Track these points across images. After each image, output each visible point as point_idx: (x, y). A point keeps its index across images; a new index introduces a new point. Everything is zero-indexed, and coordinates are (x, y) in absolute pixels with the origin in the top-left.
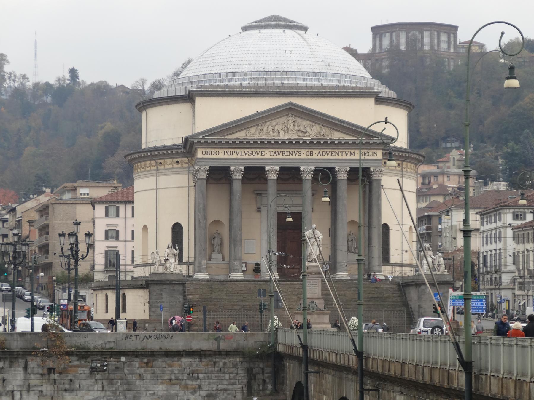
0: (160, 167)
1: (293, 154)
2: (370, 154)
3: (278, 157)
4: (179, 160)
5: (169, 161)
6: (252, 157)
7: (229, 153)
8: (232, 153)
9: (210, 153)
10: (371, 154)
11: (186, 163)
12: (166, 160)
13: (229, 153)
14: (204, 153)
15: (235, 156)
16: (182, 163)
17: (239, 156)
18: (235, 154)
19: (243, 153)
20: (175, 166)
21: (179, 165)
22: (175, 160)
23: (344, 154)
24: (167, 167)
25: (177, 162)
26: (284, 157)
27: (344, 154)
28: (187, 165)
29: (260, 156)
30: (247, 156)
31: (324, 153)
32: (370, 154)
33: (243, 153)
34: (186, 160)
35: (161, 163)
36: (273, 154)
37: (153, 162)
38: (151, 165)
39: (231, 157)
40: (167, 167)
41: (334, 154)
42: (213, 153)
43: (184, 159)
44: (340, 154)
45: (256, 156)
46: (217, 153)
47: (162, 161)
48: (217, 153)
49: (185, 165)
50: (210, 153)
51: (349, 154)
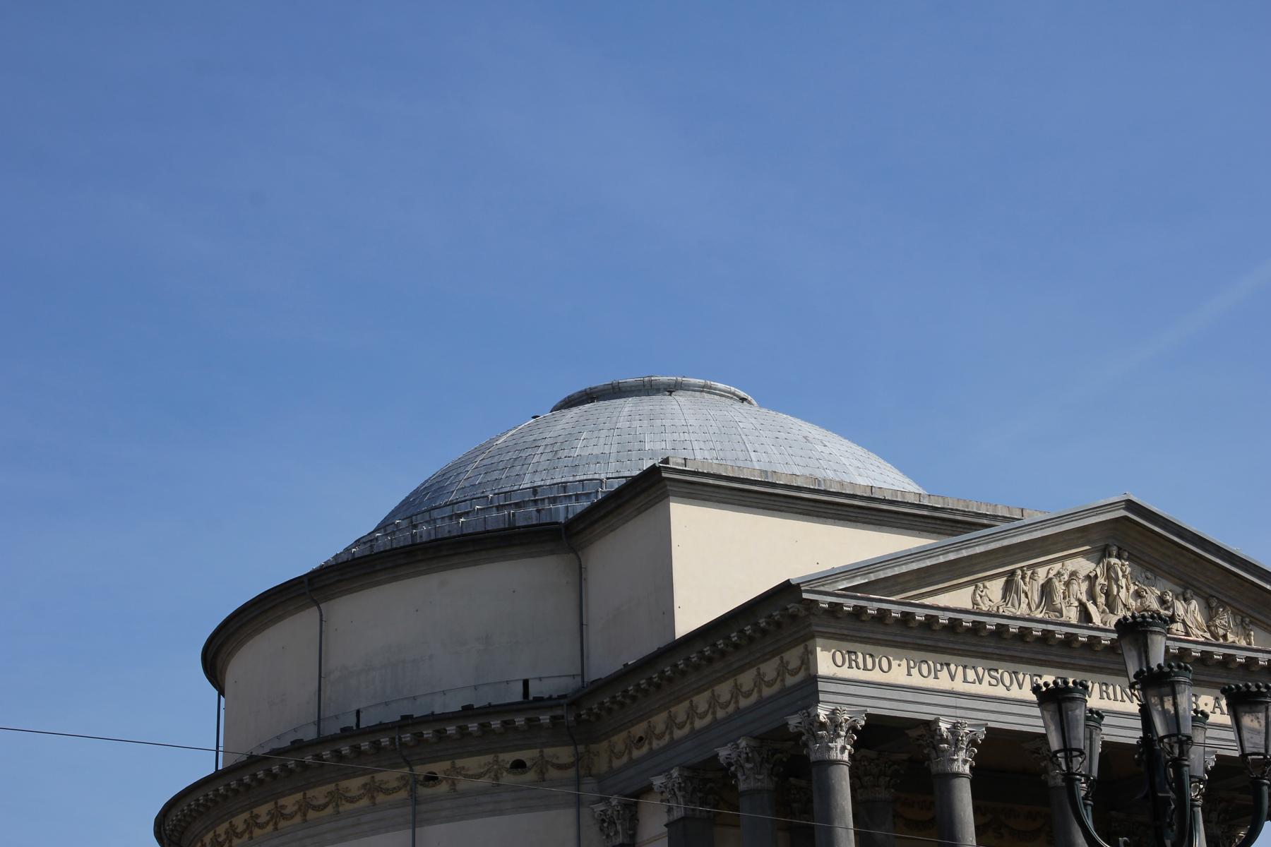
0: (424, 791)
4: (526, 755)
5: (472, 763)
11: (560, 767)
12: (460, 763)
15: (944, 682)
16: (542, 766)
20: (508, 779)
21: (531, 775)
22: (509, 757)
24: (463, 784)
25: (519, 765)
28: (571, 773)
34: (564, 754)
35: (432, 779)
37: (390, 777)
38: (372, 790)
40: (463, 784)
42: (870, 666)
43: (549, 751)
47: (438, 768)
49: (553, 773)
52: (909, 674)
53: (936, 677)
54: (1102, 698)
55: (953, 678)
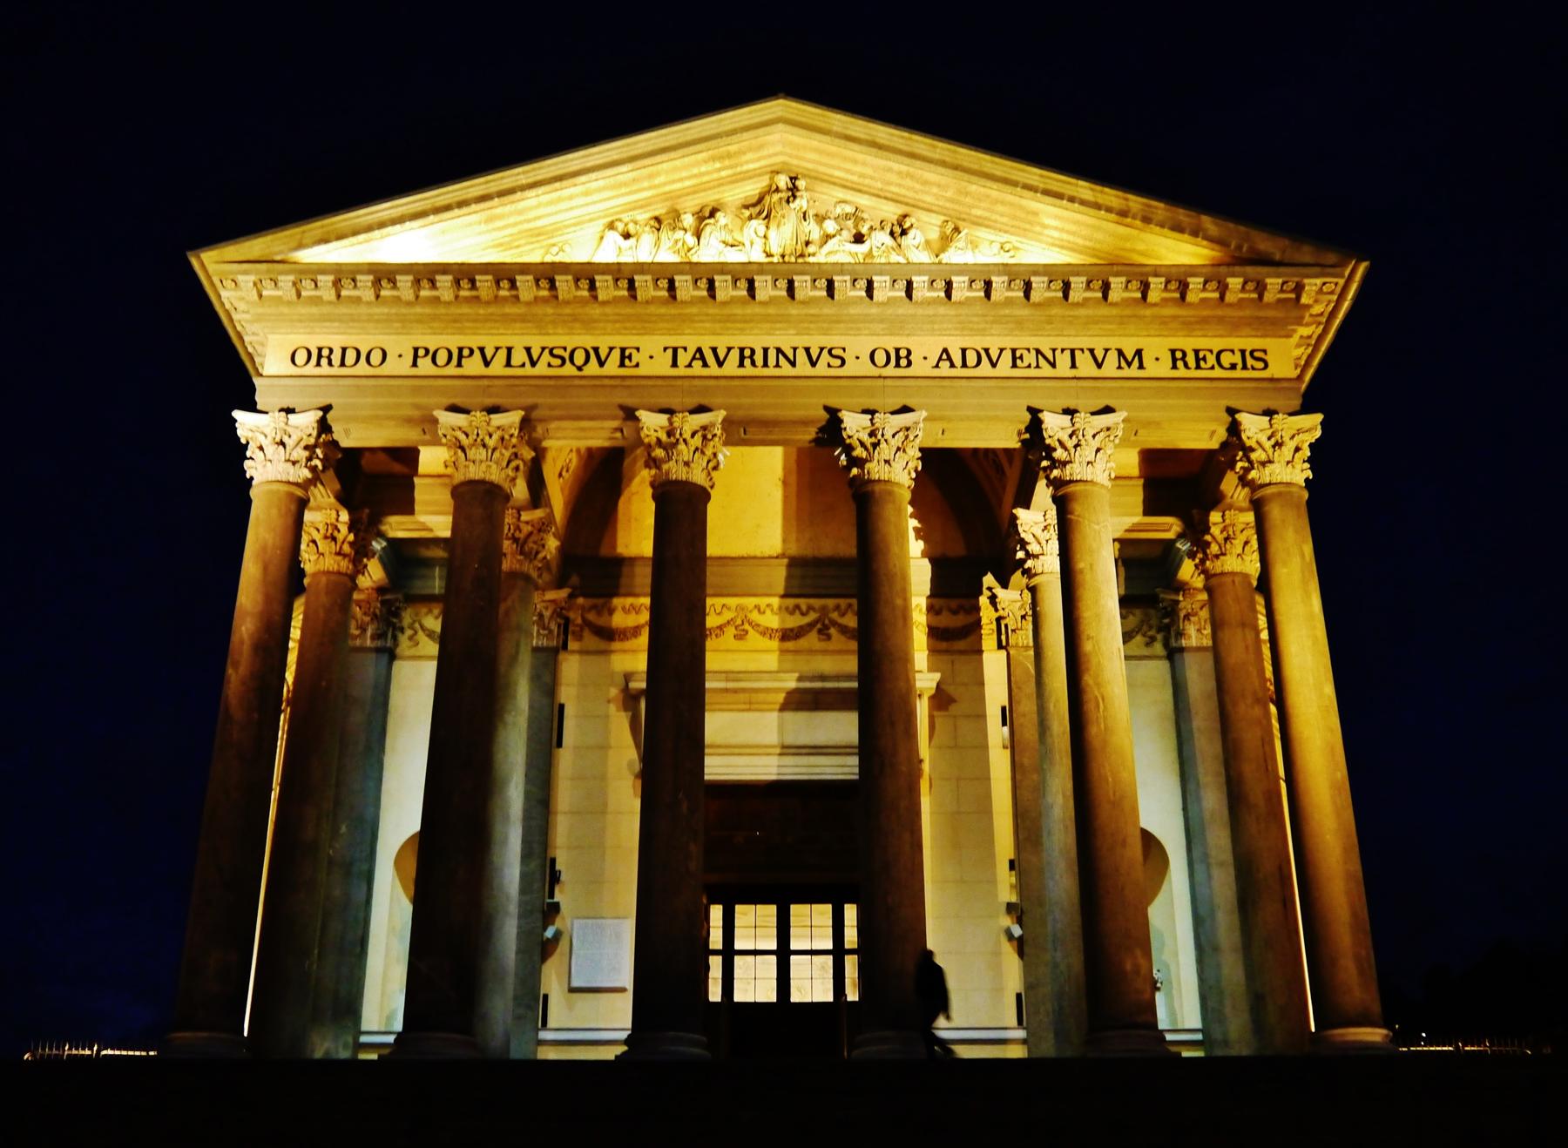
1: (801, 357)
2: (1227, 359)
3: (714, 369)
6: (569, 370)
7: (442, 357)
8: (461, 356)
9: (336, 358)
10: (1237, 359)
13: (442, 357)
14: (301, 357)
15: (473, 366)
17: (498, 367)
18: (473, 366)
19: (519, 357)
23: (1084, 360)
26: (748, 370)
27: (1084, 360)
29: (612, 367)
30: (542, 369)
31: (971, 358)
32: (1227, 359)
33: (519, 357)
36: (683, 358)
39: (452, 370)
41: (1030, 358)
44: (1063, 360)
45: (593, 368)
46: (376, 357)
48: (376, 357)
50: (336, 358)
51: (1112, 357)
52: (415, 364)
53: (459, 365)
54: (741, 365)
55: (487, 364)
